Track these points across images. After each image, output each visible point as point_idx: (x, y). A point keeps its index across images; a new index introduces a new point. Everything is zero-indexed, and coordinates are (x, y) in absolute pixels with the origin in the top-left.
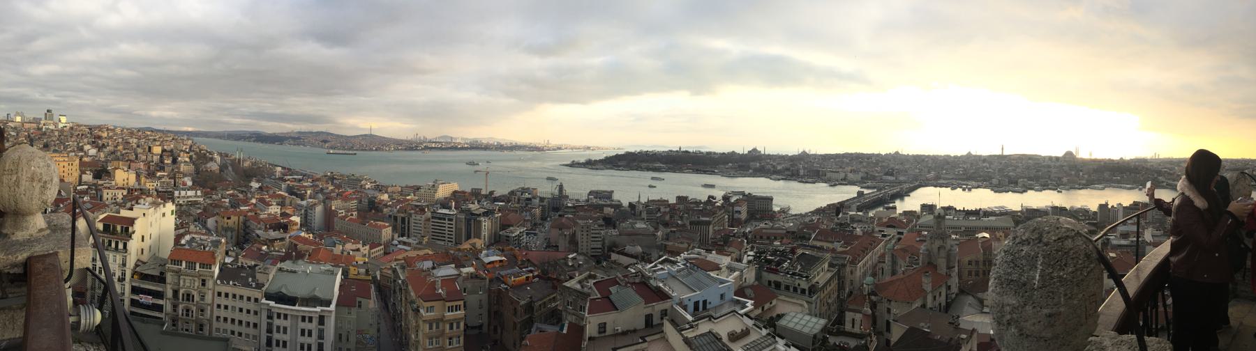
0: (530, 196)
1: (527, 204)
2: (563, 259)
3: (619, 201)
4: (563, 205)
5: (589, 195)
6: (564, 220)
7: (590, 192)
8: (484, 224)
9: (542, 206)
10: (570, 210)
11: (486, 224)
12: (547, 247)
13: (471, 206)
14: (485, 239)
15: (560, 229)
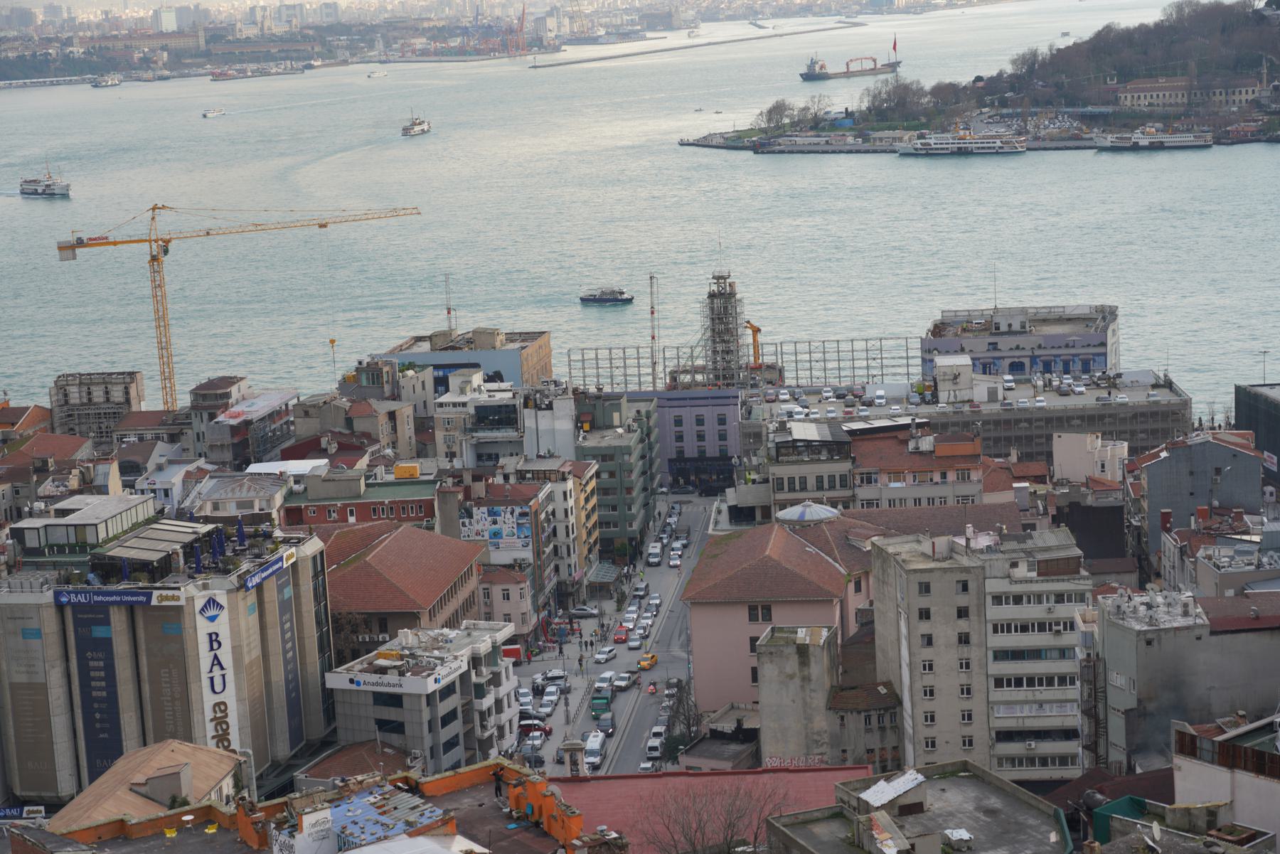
0: (502, 395)
1: (487, 457)
2: (837, 815)
3: (1169, 385)
4: (757, 436)
5: (929, 351)
6: (775, 544)
7: (938, 330)
8: (203, 627)
9: (605, 456)
10: (809, 471)
11: (222, 626)
12: (670, 750)
13: (88, 509)
14: (222, 738)
15: (760, 611)
